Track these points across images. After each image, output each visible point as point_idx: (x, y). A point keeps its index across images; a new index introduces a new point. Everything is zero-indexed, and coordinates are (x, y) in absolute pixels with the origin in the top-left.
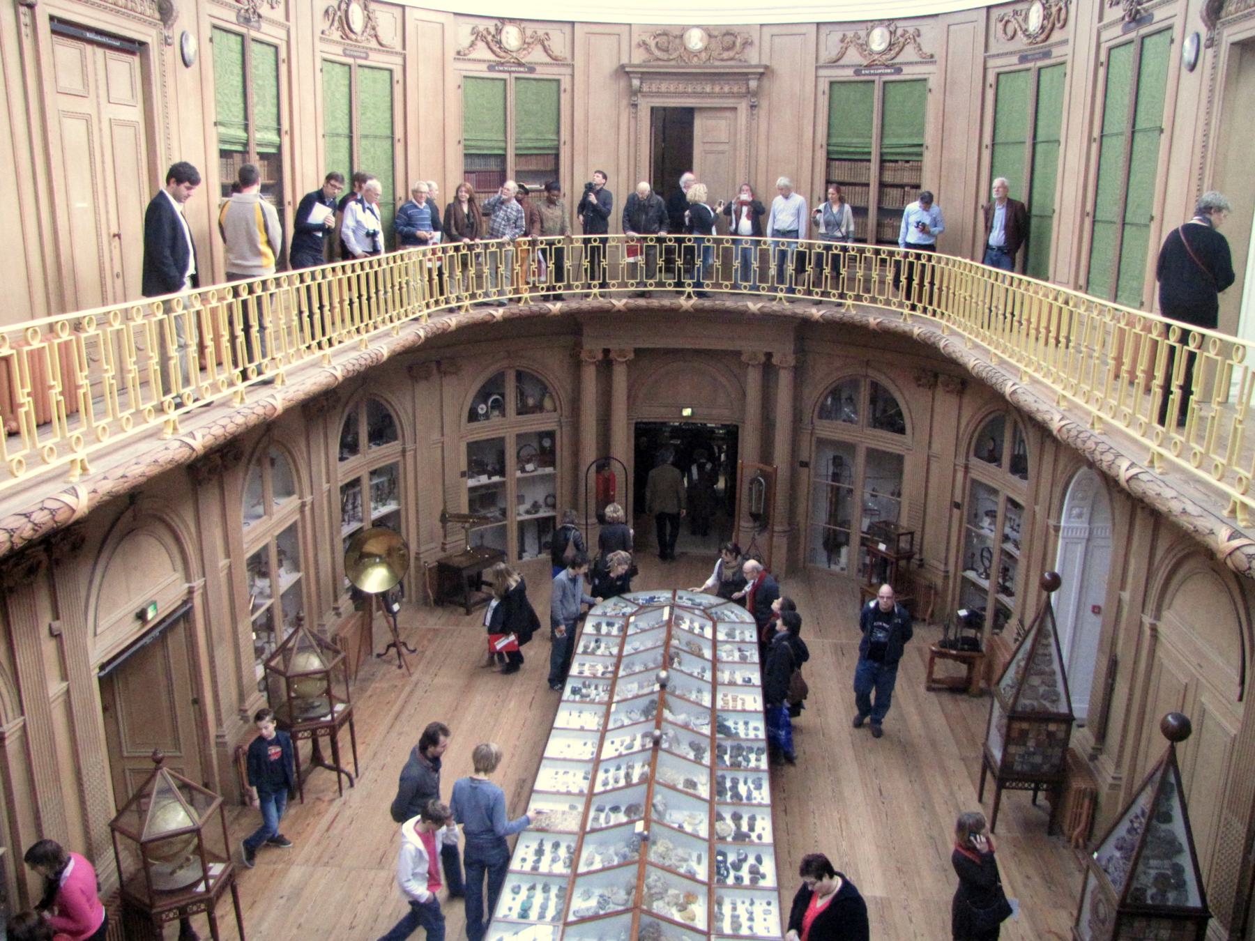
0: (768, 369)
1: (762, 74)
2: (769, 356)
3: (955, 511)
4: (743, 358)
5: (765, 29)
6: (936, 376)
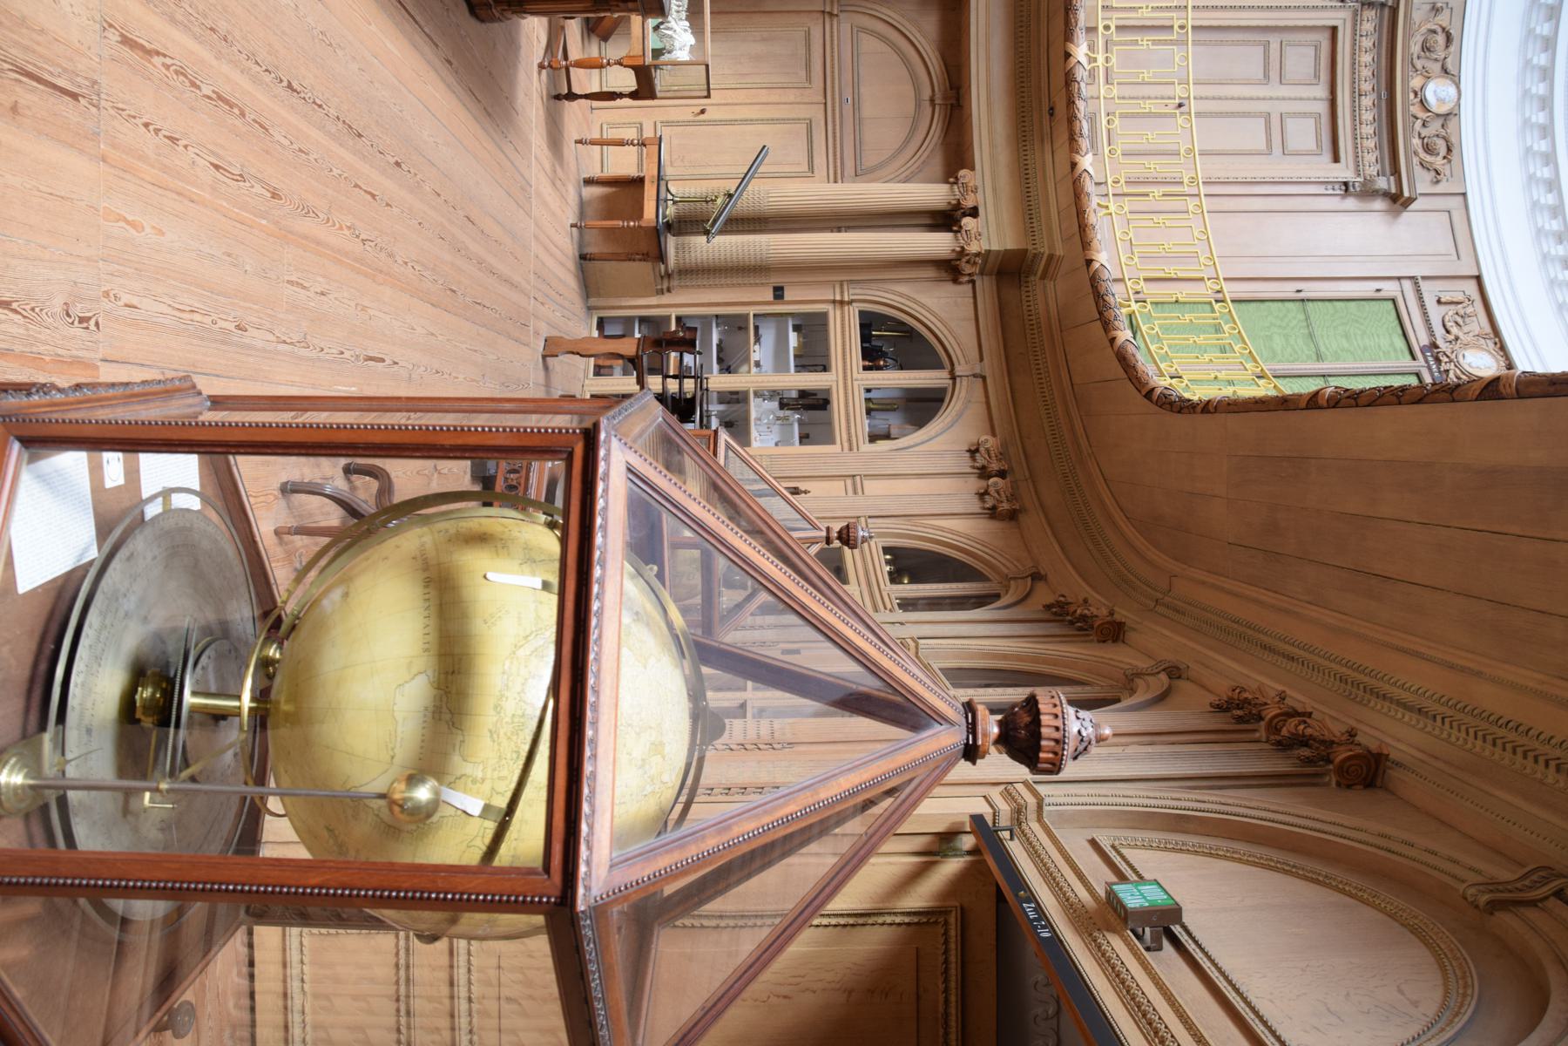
0: (945, 219)
2: (974, 212)
4: (962, 173)
6: (1002, 474)
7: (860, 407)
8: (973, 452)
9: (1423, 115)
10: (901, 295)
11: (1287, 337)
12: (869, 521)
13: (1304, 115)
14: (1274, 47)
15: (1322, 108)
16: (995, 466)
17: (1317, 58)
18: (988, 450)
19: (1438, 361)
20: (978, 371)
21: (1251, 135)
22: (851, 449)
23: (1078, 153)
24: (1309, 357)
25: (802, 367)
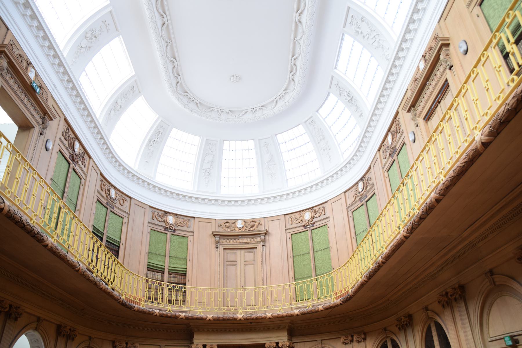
1: (266, 234)
2: (277, 343)
5: (265, 219)
6: (352, 336)
8: (346, 344)
9: (245, 228)
11: (303, 261)
13: (244, 256)
14: (228, 263)
15: (243, 251)
16: (350, 338)
17: (230, 253)
18: (345, 340)
19: (308, 225)
20: (320, 342)
21: (249, 269)
23: (266, 317)
24: (308, 255)
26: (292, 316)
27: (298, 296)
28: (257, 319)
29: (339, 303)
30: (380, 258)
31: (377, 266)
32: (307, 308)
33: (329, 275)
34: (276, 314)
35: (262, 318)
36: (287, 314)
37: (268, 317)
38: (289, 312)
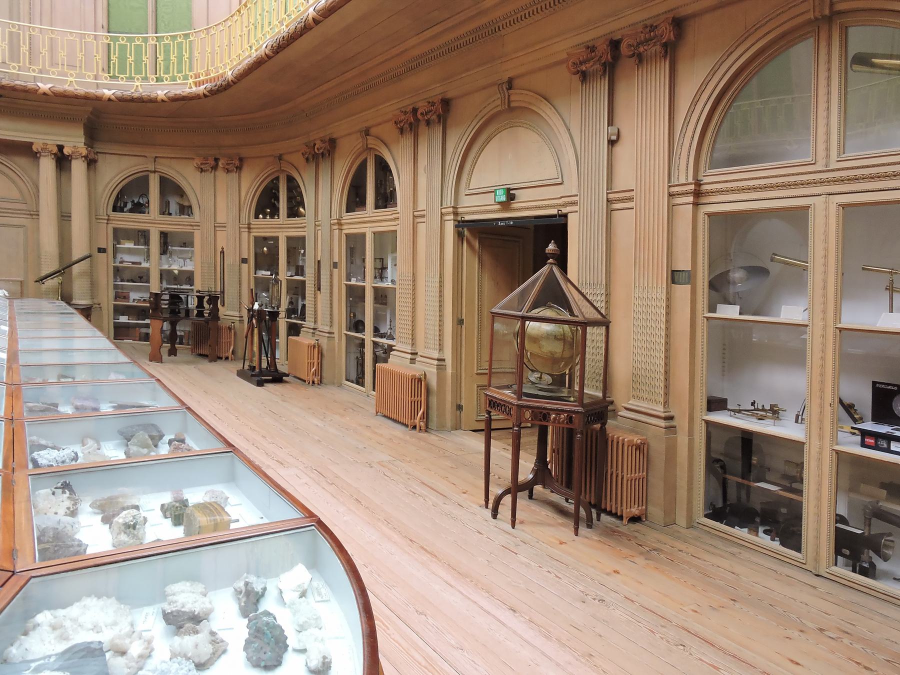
0: (62, 161)
2: (61, 148)
3: (245, 266)
4: (34, 148)
6: (216, 160)
7: (166, 218)
8: (202, 171)
10: (104, 191)
12: (241, 223)
16: (213, 163)
18: (202, 164)
20: (153, 160)
22: (199, 226)
23: (37, 90)
25: (147, 243)
26: (98, 99)
27: (114, 64)
28: (13, 89)
29: (201, 93)
30: (311, 10)
31: (299, 25)
32: (133, 91)
33: (186, 36)
34: (60, 88)
35: (26, 91)
36: (86, 93)
37: (40, 91)
38: (92, 91)
